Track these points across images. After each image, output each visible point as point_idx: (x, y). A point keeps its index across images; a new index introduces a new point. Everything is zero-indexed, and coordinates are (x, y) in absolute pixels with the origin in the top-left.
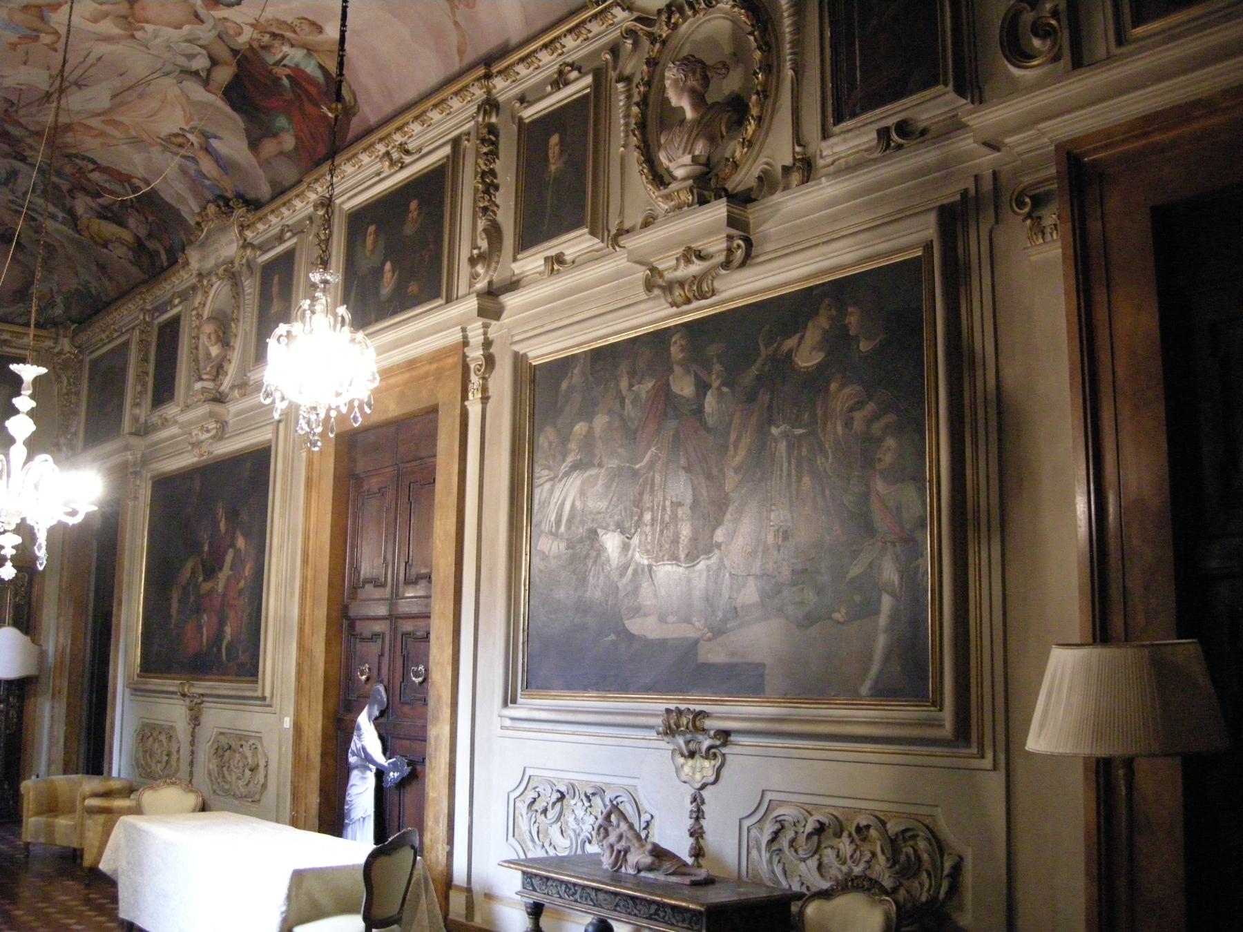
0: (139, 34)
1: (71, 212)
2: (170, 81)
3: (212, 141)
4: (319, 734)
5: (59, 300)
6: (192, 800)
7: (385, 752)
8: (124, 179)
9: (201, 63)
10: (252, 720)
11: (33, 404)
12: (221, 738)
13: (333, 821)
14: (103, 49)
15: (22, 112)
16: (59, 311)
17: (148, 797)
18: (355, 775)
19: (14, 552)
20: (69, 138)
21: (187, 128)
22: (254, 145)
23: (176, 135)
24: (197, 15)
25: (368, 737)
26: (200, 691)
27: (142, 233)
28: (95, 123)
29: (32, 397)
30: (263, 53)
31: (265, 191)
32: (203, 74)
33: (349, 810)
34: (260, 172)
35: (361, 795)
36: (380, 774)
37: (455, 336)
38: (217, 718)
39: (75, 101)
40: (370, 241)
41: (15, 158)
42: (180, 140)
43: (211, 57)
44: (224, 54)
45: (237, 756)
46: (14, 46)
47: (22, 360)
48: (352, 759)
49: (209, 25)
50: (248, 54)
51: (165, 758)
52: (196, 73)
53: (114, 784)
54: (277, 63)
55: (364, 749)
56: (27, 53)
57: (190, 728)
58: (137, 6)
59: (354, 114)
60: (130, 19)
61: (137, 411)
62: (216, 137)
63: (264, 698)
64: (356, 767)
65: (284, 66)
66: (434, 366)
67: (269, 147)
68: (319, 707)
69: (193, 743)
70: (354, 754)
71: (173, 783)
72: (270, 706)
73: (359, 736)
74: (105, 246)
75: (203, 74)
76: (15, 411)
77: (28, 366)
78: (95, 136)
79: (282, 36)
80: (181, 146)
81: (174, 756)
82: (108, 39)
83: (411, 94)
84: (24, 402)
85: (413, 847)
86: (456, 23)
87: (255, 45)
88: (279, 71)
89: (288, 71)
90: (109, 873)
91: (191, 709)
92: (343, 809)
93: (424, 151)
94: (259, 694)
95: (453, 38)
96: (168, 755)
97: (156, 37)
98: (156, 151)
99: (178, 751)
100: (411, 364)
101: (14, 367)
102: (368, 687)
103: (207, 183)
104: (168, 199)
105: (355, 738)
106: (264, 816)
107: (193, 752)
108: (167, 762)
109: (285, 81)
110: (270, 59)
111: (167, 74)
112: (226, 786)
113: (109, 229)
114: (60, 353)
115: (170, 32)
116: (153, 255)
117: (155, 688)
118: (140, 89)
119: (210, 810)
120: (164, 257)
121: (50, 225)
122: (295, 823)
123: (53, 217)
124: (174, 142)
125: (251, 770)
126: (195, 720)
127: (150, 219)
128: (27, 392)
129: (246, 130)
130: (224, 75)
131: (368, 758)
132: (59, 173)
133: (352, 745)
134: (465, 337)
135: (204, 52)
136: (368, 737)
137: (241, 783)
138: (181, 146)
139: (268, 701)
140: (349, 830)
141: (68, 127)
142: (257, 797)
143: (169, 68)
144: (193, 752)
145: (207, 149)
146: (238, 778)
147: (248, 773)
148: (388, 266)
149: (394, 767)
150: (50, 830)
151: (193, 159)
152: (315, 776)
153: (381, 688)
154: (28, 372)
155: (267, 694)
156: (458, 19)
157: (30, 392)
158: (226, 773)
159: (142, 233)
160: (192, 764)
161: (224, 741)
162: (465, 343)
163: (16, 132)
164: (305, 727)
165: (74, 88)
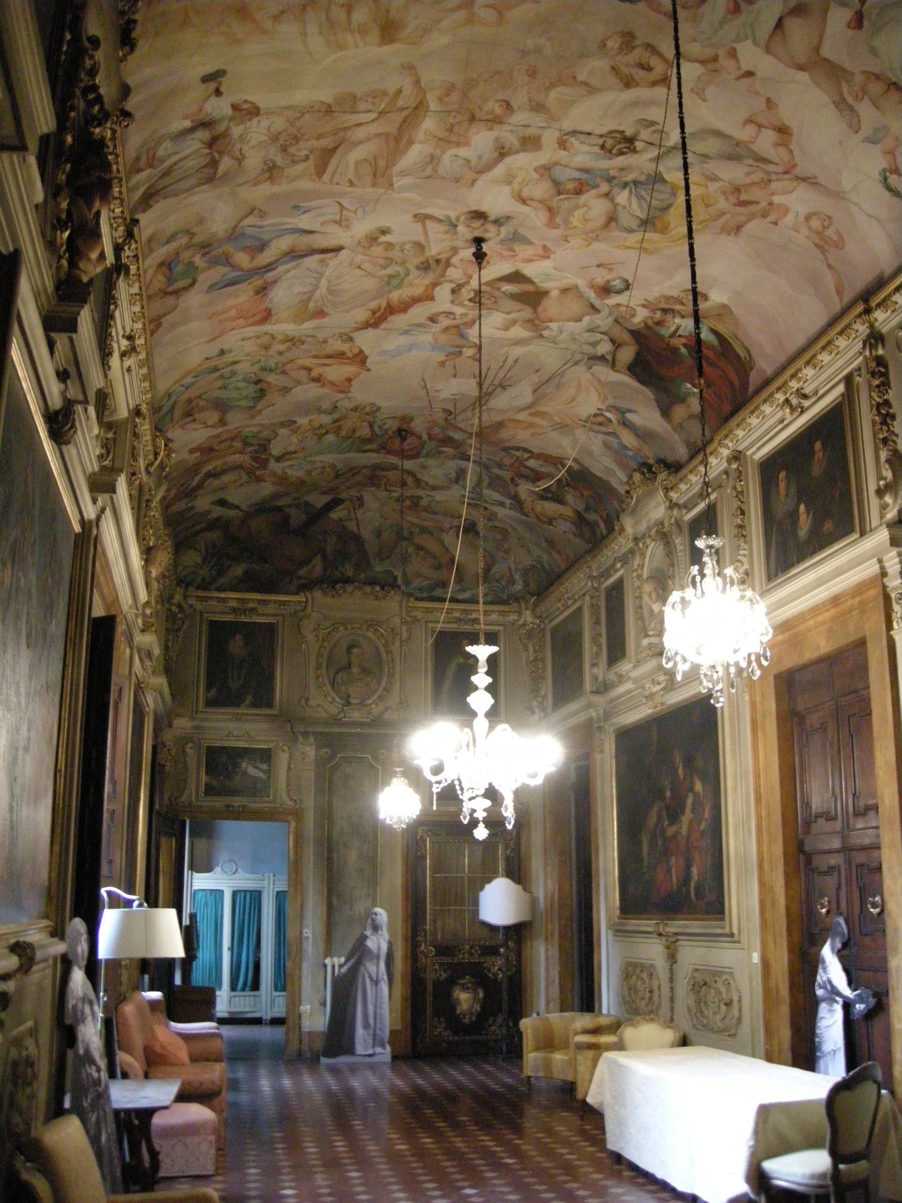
0: (546, 333)
1: (515, 498)
2: (581, 368)
3: (629, 416)
4: (786, 968)
5: (517, 577)
6: (670, 1035)
7: (850, 983)
8: (557, 461)
9: (605, 348)
10: (724, 956)
11: (489, 680)
12: (696, 974)
13: (805, 1056)
14: (518, 351)
15: (460, 418)
16: (519, 586)
17: (629, 1033)
18: (823, 1008)
19: (485, 814)
20: (504, 434)
21: (603, 407)
22: (666, 413)
23: (595, 415)
24: (593, 307)
25: (833, 971)
26: (674, 930)
27: (580, 507)
28: (522, 416)
29: (487, 673)
30: (657, 328)
31: (682, 452)
32: (609, 358)
33: (820, 1043)
34: (676, 436)
35: (831, 1027)
36: (847, 1006)
37: (870, 569)
38: (692, 955)
39: (501, 401)
40: (782, 485)
41: (461, 458)
42: (600, 419)
43: (613, 341)
44: (626, 337)
45: (712, 991)
46: (442, 364)
47: (475, 641)
48: (820, 992)
49: (605, 312)
50: (644, 332)
51: (648, 995)
52: (602, 358)
53: (603, 1021)
54: (672, 336)
55: (830, 982)
56: (455, 368)
57: (667, 965)
58: (540, 309)
59: (752, 369)
60: (536, 322)
61: (595, 670)
62: (630, 411)
63: (732, 935)
64: (824, 1000)
65: (680, 336)
66: (858, 599)
67: (679, 412)
68: (783, 942)
69: (671, 980)
70: (821, 987)
71: (652, 1020)
72: (738, 942)
73: (825, 969)
74: (550, 523)
75: (609, 358)
76: (476, 688)
77: (481, 646)
78: (525, 428)
79: (673, 310)
80: (600, 424)
81: (656, 993)
82: (519, 342)
83: (800, 340)
84: (481, 679)
85: (875, 1082)
86: (829, 266)
87: (650, 322)
89: (684, 340)
90: (596, 1106)
91: (668, 948)
92: (813, 1042)
93: (821, 393)
94: (727, 931)
95: (829, 281)
96: (650, 992)
97: (561, 333)
98: (579, 432)
99: (659, 988)
100: (835, 600)
101: (470, 649)
102: (828, 920)
103: (630, 453)
104: (598, 474)
105: (820, 971)
106: (739, 1050)
107: (672, 989)
108: (651, 998)
109: (683, 350)
110: (665, 332)
111: (577, 363)
112: (702, 1024)
113: (551, 508)
114: (524, 624)
115: (571, 326)
116: (593, 526)
117: (634, 928)
118: (557, 380)
119: (691, 1045)
120: (602, 526)
121: (501, 512)
122: (770, 1057)
123: (502, 504)
124: (597, 422)
125: (726, 1005)
126: (672, 958)
127: (586, 493)
128: (483, 668)
129: (657, 400)
130: (627, 354)
131: (834, 991)
132: (500, 466)
133: (818, 978)
134: (882, 568)
135: (605, 338)
136: (833, 971)
137: (718, 1017)
138: (600, 424)
139: (736, 938)
140: (821, 1064)
141: (500, 425)
142: (733, 1032)
143: (578, 357)
144: (672, 989)
145: (625, 423)
146: (715, 1013)
147: (723, 1008)
148: (802, 508)
149: (860, 999)
150: (548, 1065)
151: (614, 434)
152: (785, 1009)
153: (841, 921)
154: (482, 652)
155: (735, 931)
156: (831, 262)
157: (485, 669)
158: (704, 1009)
159: (580, 507)
160: (672, 1000)
161: (699, 977)
162: (884, 574)
163: (457, 436)
164: (772, 962)
165: (499, 390)
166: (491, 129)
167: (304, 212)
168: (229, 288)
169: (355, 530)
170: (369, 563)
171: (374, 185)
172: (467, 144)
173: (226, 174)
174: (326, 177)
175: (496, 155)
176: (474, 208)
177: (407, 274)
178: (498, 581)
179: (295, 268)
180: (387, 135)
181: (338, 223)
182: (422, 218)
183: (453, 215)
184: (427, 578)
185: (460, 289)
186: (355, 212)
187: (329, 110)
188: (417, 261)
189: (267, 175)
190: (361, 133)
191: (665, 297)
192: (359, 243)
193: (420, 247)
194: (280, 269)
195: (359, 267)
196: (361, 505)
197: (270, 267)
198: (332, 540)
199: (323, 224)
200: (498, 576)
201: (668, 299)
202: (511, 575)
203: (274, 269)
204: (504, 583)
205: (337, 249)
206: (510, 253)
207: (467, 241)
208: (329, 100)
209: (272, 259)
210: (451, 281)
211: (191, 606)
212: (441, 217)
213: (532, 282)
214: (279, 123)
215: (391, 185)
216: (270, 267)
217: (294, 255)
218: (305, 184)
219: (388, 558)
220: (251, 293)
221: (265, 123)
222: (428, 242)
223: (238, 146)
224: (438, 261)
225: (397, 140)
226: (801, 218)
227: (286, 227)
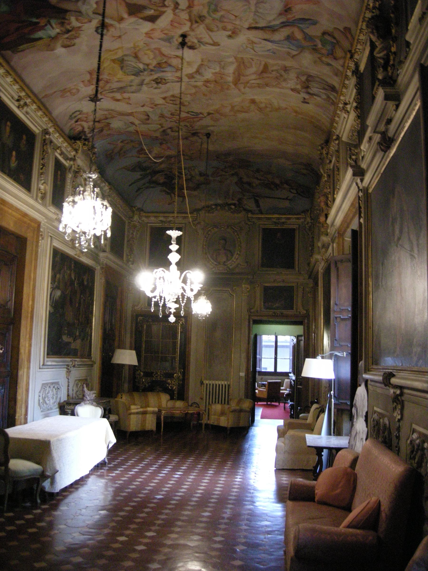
66: (29, 222)
79: (67, 33)
86: (55, 92)
88: (43, 22)
100: (25, 215)
109: (35, 20)
166: (207, 79)
167: (270, 50)
168: (306, 17)
171: (242, 58)
172: (213, 73)
173: (303, 75)
174: (263, 63)
175: (200, 71)
176: (195, 51)
177: (208, 12)
179: (270, 22)
180: (244, 76)
181: (253, 42)
182: (215, 44)
183: (202, 46)
185: (175, 6)
186: (247, 47)
187: (267, 85)
188: (207, 21)
189: (287, 69)
190: (253, 77)
191: (78, 37)
192: (240, 31)
193: (209, 29)
194: (277, 22)
195: (236, 16)
197: (284, 25)
199: (261, 43)
201: (76, 37)
203: (282, 23)
205: (250, 28)
206: (165, 32)
207: (189, 35)
208: (267, 88)
209: (282, 30)
210: (183, 10)
212: (207, 45)
213: (142, 18)
214: (284, 84)
215: (235, 58)
216: (284, 25)
217: (270, 29)
218: (271, 61)
220: (294, 10)
221: (289, 85)
222: (207, 33)
223: (298, 82)
224: (196, 22)
225: (239, 75)
226: (79, 88)
227: (278, 45)
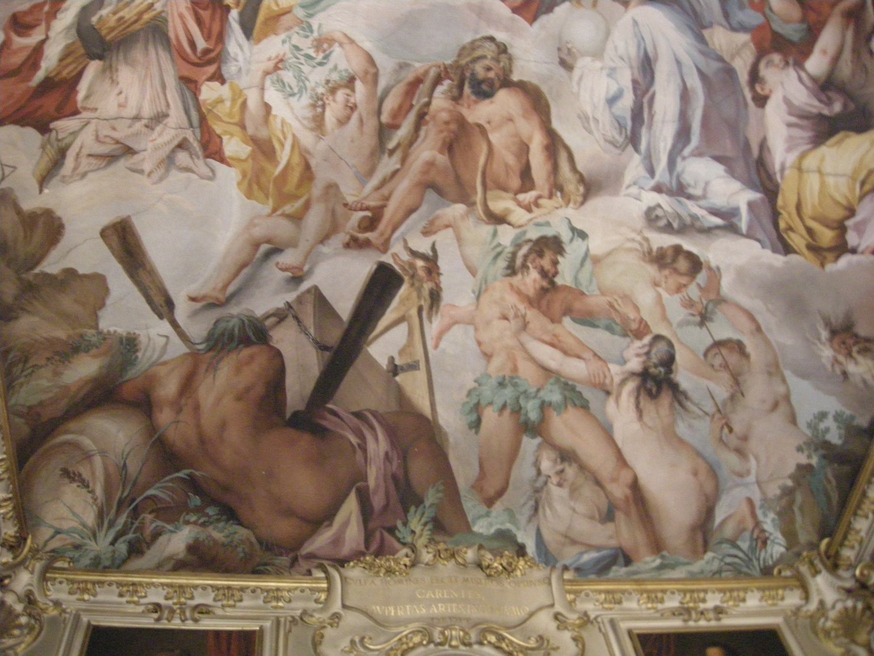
74: (841, 248)
169: (427, 411)
170: (462, 514)
178: (733, 543)
184: (590, 547)
196: (435, 297)
198: (378, 446)
200: (729, 531)
202: (757, 524)
204: (745, 545)
211: (57, 604)
219: (500, 493)
